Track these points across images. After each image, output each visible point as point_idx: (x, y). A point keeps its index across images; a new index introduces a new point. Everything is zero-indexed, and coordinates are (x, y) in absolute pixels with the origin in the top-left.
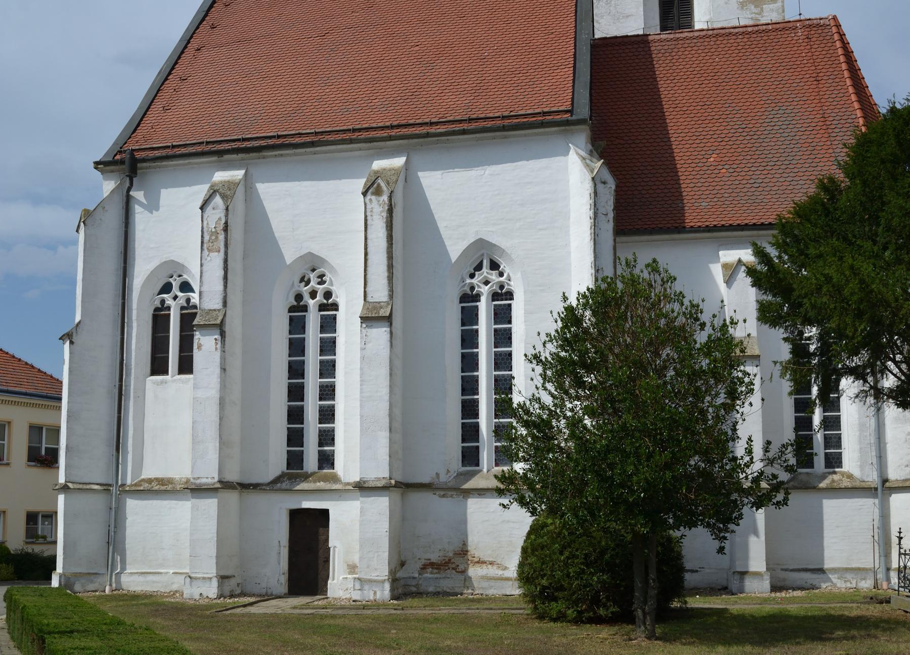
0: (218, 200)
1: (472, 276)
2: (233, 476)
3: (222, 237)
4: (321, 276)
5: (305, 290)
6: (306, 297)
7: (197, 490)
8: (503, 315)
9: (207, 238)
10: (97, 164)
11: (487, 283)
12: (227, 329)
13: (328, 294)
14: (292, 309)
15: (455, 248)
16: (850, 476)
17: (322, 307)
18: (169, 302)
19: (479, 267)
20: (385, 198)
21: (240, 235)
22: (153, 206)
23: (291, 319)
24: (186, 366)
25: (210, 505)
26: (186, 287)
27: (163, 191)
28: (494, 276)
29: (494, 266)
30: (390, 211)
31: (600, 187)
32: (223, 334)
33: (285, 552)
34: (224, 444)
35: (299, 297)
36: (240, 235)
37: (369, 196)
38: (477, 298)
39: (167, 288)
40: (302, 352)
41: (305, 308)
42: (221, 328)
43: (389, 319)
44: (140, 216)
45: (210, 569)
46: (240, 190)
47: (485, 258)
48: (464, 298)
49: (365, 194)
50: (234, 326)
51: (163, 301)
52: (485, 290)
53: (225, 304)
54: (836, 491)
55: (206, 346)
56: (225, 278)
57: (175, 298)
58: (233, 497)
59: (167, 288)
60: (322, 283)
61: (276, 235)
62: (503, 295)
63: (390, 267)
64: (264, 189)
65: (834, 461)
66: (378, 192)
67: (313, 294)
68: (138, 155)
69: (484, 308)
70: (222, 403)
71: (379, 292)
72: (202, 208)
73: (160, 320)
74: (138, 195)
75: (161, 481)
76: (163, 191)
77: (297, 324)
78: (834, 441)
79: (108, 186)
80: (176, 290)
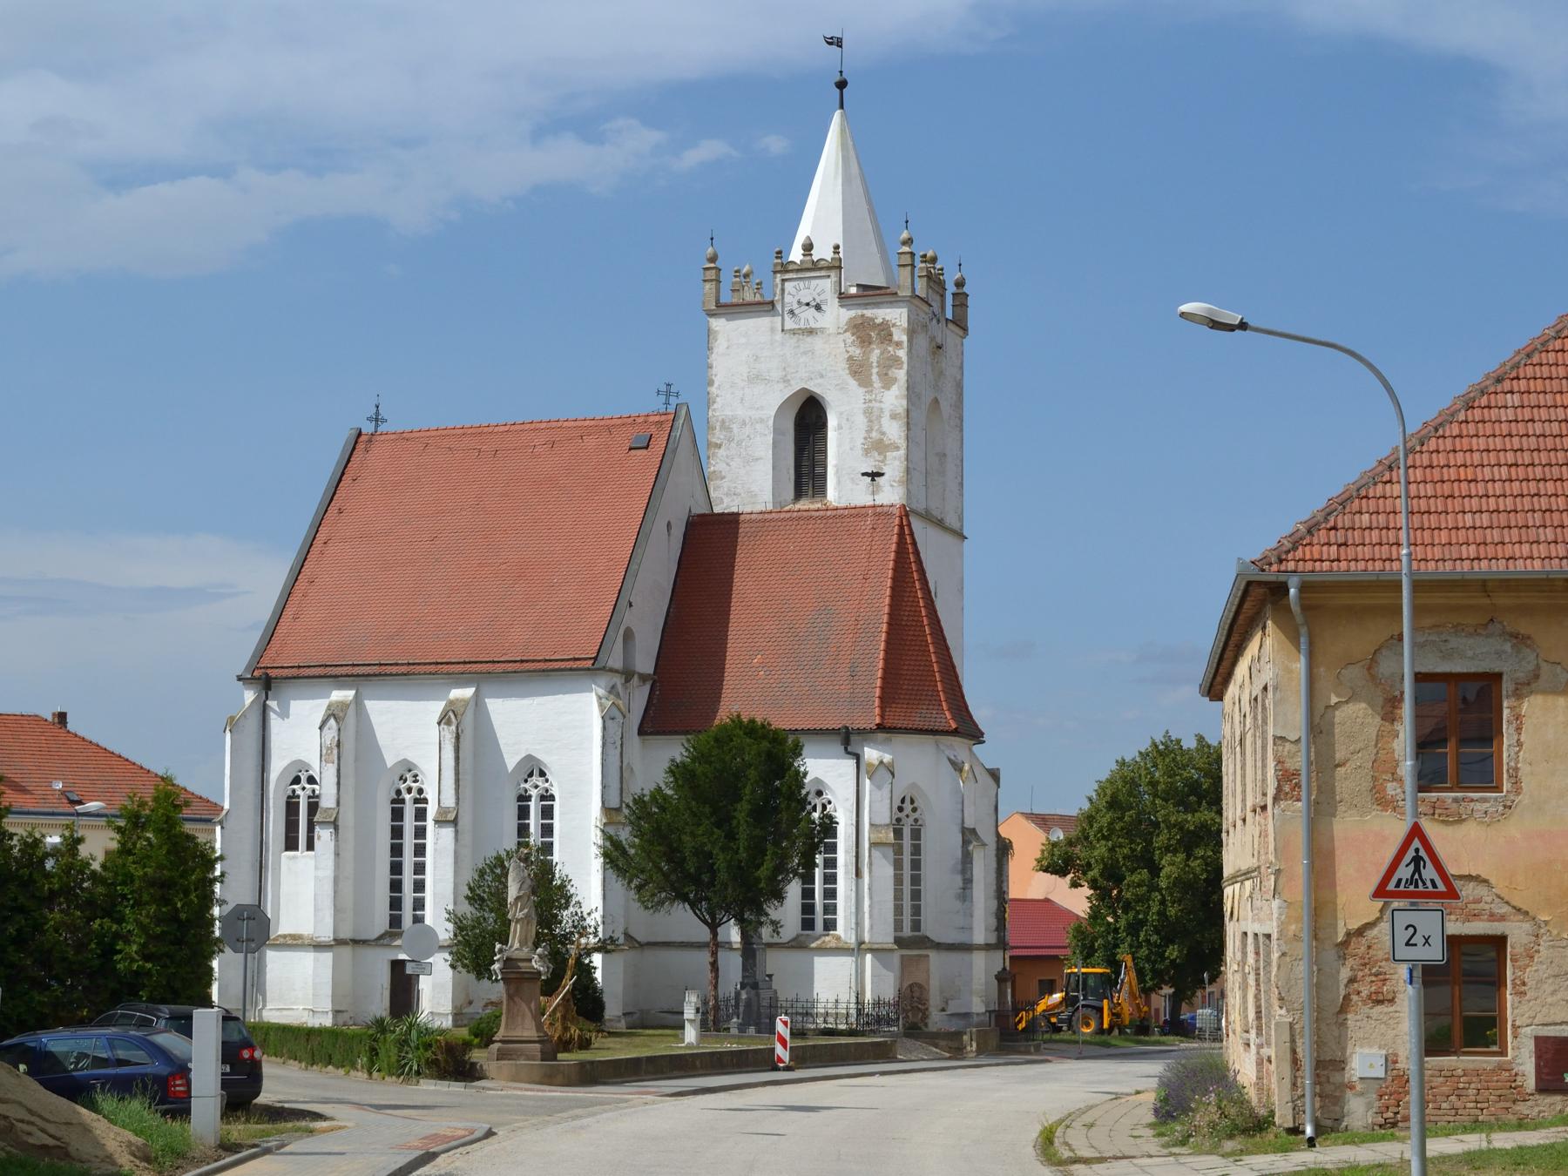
0: (332, 721)
2: (346, 934)
3: (335, 751)
5: (403, 787)
6: (404, 792)
7: (319, 947)
8: (547, 812)
12: (340, 823)
13: (420, 791)
14: (393, 802)
15: (511, 762)
16: (838, 938)
17: (416, 801)
18: (299, 792)
19: (531, 775)
20: (453, 728)
21: (351, 740)
22: (284, 714)
25: (327, 957)
26: (311, 780)
27: (292, 703)
28: (540, 781)
29: (542, 774)
30: (458, 737)
31: (609, 723)
32: (336, 828)
33: (387, 994)
34: (337, 910)
35: (399, 792)
36: (351, 740)
38: (529, 798)
39: (297, 780)
40: (401, 837)
41: (403, 801)
42: (335, 825)
43: (455, 822)
44: (275, 721)
45: (327, 1005)
46: (351, 711)
47: (534, 769)
50: (348, 819)
52: (534, 793)
53: (338, 803)
54: (825, 951)
55: (324, 835)
56: (338, 783)
58: (347, 951)
59: (297, 780)
61: (381, 743)
62: (547, 797)
63: (457, 781)
64: (370, 705)
65: (830, 925)
66: (449, 723)
67: (409, 790)
68: (273, 673)
69: (534, 807)
70: (336, 880)
71: (449, 801)
72: (321, 728)
73: (292, 807)
74: (272, 704)
75: (293, 937)
76: (292, 703)
77: (397, 814)
78: (830, 909)
79: (249, 696)
80: (304, 782)
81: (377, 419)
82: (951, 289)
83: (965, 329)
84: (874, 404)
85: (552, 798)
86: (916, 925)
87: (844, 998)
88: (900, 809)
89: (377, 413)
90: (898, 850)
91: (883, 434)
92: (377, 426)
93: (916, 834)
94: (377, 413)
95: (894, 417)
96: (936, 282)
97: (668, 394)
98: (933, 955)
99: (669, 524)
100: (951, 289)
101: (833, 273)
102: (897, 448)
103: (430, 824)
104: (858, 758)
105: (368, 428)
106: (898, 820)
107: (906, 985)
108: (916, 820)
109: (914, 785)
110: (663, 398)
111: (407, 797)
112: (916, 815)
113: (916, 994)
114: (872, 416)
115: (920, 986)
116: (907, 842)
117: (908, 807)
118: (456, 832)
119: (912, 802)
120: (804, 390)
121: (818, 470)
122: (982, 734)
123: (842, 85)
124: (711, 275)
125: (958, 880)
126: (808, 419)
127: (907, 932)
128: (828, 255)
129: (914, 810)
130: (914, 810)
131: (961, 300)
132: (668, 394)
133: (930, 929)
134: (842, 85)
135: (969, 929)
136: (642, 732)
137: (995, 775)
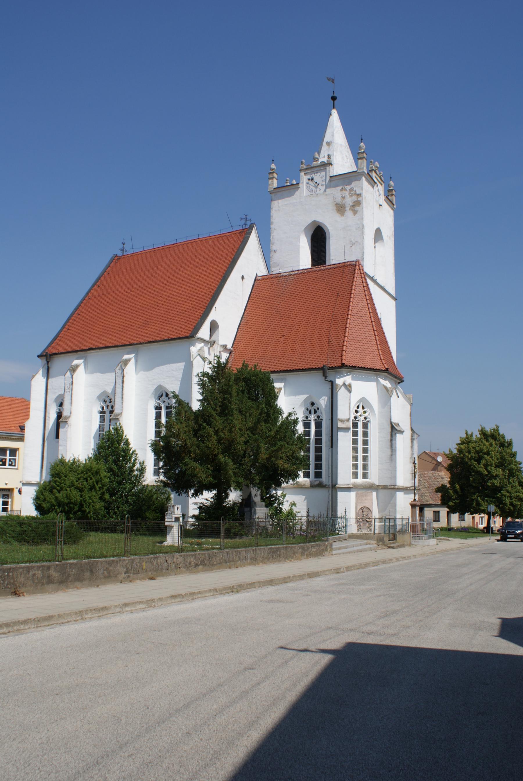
4: (110, 399)
10: (39, 356)
11: (164, 402)
13: (112, 407)
14: (101, 413)
19: (162, 396)
28: (166, 399)
35: (103, 408)
38: (160, 408)
52: (163, 406)
81: (123, 250)
86: (365, 476)
88: (357, 412)
89: (123, 247)
90: (355, 434)
92: (123, 253)
93: (365, 426)
94: (123, 247)
97: (246, 220)
99: (243, 278)
104: (332, 383)
105: (120, 254)
106: (355, 418)
107: (359, 508)
108: (365, 418)
109: (363, 400)
110: (243, 222)
112: (366, 415)
113: (365, 513)
116: (360, 429)
117: (360, 410)
119: (363, 408)
120: (314, 222)
123: (334, 98)
125: (389, 452)
126: (318, 238)
127: (360, 480)
128: (325, 160)
132: (246, 220)
134: (334, 98)
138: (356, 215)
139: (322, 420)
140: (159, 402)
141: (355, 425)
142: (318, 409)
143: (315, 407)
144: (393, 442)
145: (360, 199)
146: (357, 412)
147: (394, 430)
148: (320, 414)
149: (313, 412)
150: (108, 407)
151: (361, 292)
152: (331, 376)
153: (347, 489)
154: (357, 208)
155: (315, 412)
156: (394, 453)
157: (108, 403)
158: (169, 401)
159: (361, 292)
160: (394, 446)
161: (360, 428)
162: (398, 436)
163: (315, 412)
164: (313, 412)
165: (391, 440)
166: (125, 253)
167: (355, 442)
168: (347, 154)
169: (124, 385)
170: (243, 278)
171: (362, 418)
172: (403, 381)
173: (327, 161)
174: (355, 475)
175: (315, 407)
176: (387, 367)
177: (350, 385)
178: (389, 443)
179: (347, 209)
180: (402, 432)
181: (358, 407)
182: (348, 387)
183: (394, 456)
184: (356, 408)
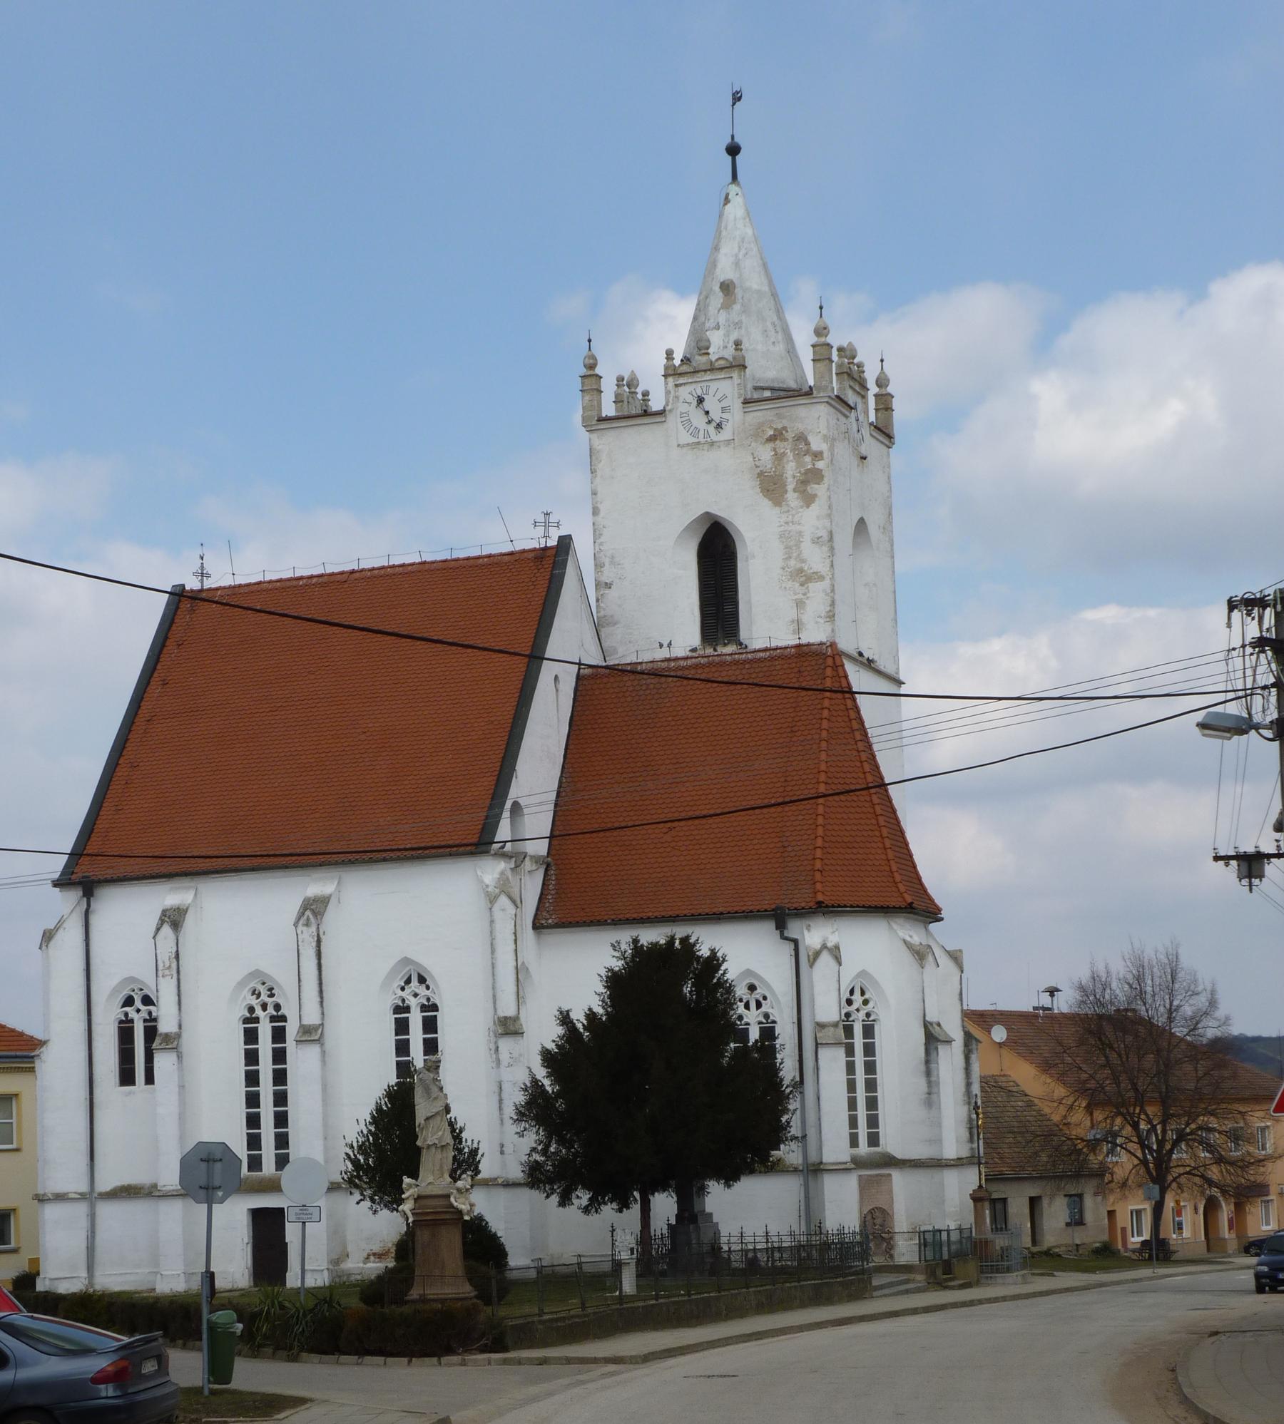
1: (403, 989)
4: (271, 989)
8: (430, 1025)
9: (161, 967)
10: (57, 884)
11: (416, 995)
13: (277, 1007)
14: (246, 1021)
19: (408, 981)
20: (313, 929)
23: (246, 1030)
24: (150, 1079)
26: (147, 1000)
28: (422, 991)
29: (422, 980)
35: (251, 1010)
37: (300, 928)
38: (407, 1009)
39: (129, 1001)
41: (257, 1020)
48: (397, 1009)
49: (296, 925)
51: (126, 1014)
52: (413, 1003)
57: (138, 1011)
60: (272, 996)
66: (307, 924)
72: (154, 938)
73: (125, 1033)
80: (138, 1003)
81: (202, 574)
82: (873, 389)
83: (890, 437)
84: (791, 527)
85: (434, 1007)
86: (874, 1140)
87: (795, 1228)
90: (850, 1051)
91: (803, 561)
93: (868, 1031)
95: (816, 541)
96: (853, 376)
97: (547, 525)
98: (897, 1176)
99: (556, 677)
100: (873, 389)
101: (735, 374)
102: (822, 578)
103: (290, 1044)
105: (192, 584)
108: (868, 1015)
109: (863, 974)
110: (540, 531)
111: (259, 1012)
113: (878, 1221)
114: (791, 543)
115: (883, 1211)
117: (857, 998)
118: (323, 1053)
119: (863, 993)
120: (707, 513)
121: (728, 609)
122: (940, 910)
124: (591, 383)
125: (922, 1082)
126: (717, 551)
127: (863, 1149)
128: (729, 353)
129: (866, 1002)
130: (866, 1002)
131: (885, 403)
132: (547, 525)
133: (894, 1141)
135: (938, 1141)
136: (537, 926)
137: (956, 957)
138: (813, 506)
139: (774, 1022)
140: (403, 994)
141: (849, 1031)
142: (765, 998)
143: (758, 994)
144: (933, 1066)
145: (820, 465)
146: (849, 1002)
147: (932, 1038)
148: (770, 1011)
149: (753, 1005)
150: (264, 1007)
151: (843, 724)
152: (794, 928)
153: (841, 1169)
154: (813, 488)
155: (759, 1005)
156: (934, 1090)
157: (264, 997)
158: (428, 993)
159: (843, 724)
160: (934, 1073)
161: (855, 1033)
162: (942, 1049)
163: (759, 1005)
164: (753, 1005)
165: (927, 1062)
166: (209, 584)
167: (850, 1068)
168: (775, 318)
169: (323, 962)
170: (556, 677)
171: (862, 1015)
172: (942, 919)
173: (734, 358)
174: (854, 1142)
175: (758, 994)
176: (909, 900)
177: (837, 948)
178: (923, 1068)
179: (790, 487)
180: (949, 1042)
181: (852, 992)
182: (836, 953)
183: (934, 1097)
184: (848, 995)
